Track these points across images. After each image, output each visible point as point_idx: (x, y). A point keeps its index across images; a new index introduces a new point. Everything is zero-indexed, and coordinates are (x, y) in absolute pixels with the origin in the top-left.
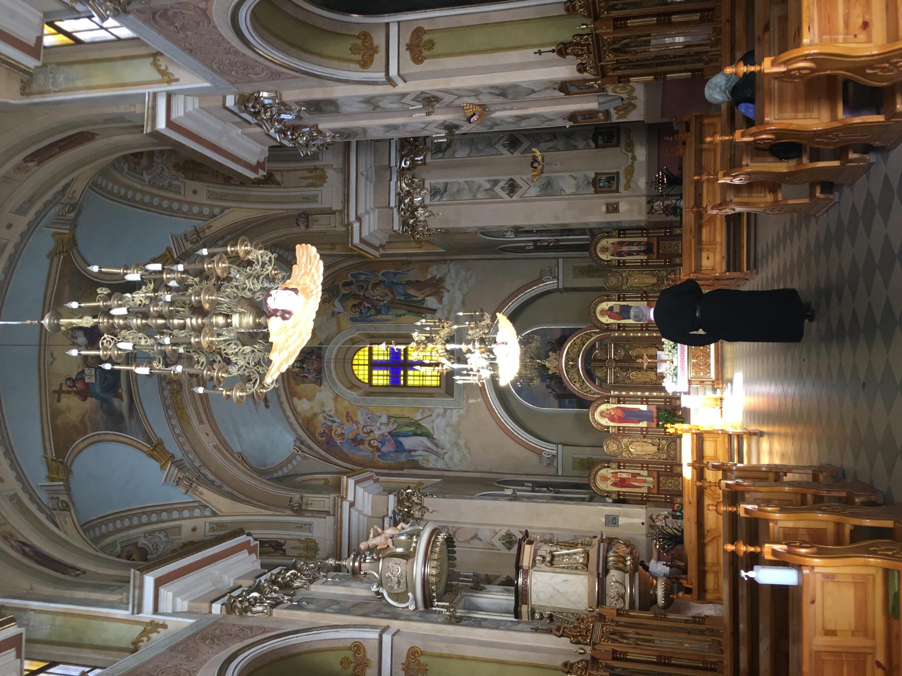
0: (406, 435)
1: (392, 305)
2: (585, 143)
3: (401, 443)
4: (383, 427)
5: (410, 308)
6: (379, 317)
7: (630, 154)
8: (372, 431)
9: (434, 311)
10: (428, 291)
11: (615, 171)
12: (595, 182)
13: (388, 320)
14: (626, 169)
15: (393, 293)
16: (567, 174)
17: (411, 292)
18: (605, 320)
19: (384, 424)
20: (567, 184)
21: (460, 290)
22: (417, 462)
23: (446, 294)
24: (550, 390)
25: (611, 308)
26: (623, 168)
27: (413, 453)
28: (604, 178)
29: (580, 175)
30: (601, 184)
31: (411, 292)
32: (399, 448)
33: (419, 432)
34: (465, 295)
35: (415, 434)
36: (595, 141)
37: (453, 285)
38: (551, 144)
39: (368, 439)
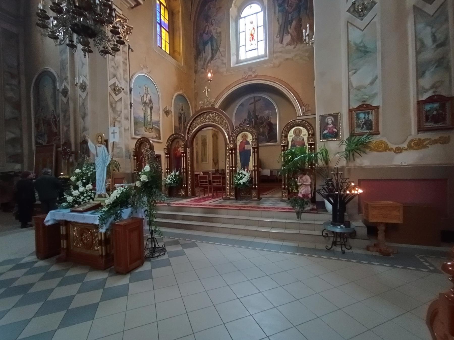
0: (212, 45)
1: (285, 13)
2: (427, 86)
3: (208, 43)
4: (215, 31)
5: (283, 26)
6: (277, 7)
7: (405, 146)
8: (212, 25)
9: (281, 42)
10: (295, 34)
11: (381, 129)
12: (366, 107)
13: (275, 14)
14: (382, 142)
15: (293, 10)
16: (378, 72)
17: (294, 23)
18: (239, 139)
19: (216, 31)
20: (362, 77)
21: (296, 55)
22: (200, 55)
23: (293, 46)
24: (243, 121)
25: (248, 143)
26: (385, 139)
27: (203, 52)
28: (371, 117)
29: (377, 88)
30: (362, 116)
31: (294, 23)
32: (205, 44)
33: (214, 52)
34: (292, 59)
35: (212, 50)
36: (430, 100)
37: (299, 50)
38: (428, 42)
39: (209, 24)
